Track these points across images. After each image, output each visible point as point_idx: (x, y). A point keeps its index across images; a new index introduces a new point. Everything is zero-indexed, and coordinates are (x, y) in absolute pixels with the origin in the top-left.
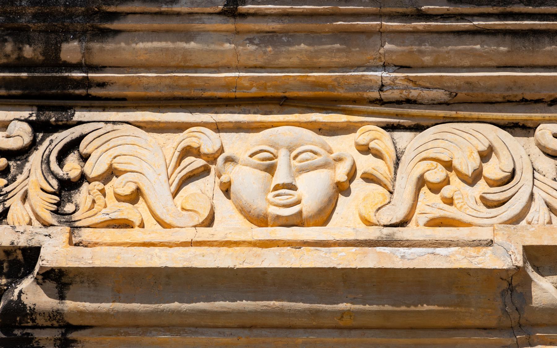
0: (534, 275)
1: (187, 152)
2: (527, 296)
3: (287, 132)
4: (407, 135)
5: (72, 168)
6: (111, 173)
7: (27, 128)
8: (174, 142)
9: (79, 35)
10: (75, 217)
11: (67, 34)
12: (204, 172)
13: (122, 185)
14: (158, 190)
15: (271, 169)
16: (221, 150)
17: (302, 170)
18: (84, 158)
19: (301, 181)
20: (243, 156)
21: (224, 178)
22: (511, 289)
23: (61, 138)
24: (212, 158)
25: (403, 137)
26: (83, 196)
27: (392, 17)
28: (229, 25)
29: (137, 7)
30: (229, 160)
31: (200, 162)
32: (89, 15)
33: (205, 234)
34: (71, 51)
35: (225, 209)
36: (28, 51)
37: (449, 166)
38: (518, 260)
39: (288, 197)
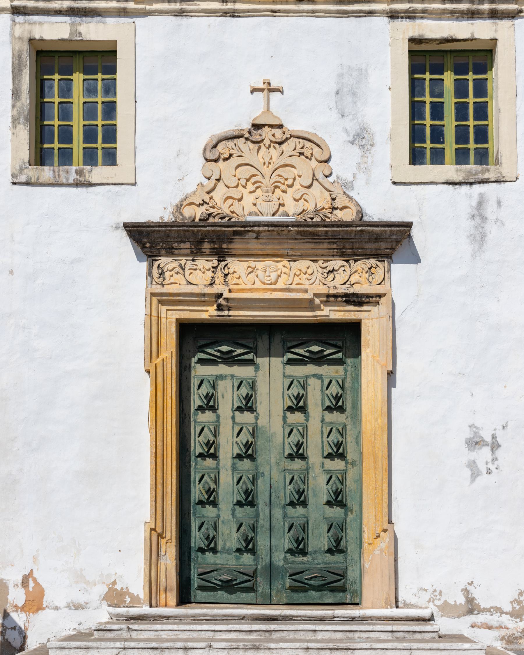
0: (315, 298)
1: (249, 267)
2: (314, 302)
3: (269, 263)
4: (293, 262)
5: (226, 271)
6: (234, 272)
7: (217, 261)
8: (246, 264)
9: (226, 243)
10: (228, 282)
11: (223, 242)
12: (252, 272)
13: (236, 275)
14: (243, 276)
15: (265, 272)
16: (256, 267)
17: (272, 272)
18: (229, 268)
19: (272, 274)
20: (260, 268)
21: (256, 274)
22: (311, 301)
23: (224, 263)
24: (254, 269)
25: (292, 263)
26: (229, 277)
27: (290, 239)
28: (257, 241)
29: (237, 237)
30: (257, 269)
31: (251, 270)
32: (228, 239)
33: (253, 287)
34: (224, 246)
35: (257, 280)
36: (216, 246)
37: (301, 270)
38: (312, 296)
39: (269, 278)
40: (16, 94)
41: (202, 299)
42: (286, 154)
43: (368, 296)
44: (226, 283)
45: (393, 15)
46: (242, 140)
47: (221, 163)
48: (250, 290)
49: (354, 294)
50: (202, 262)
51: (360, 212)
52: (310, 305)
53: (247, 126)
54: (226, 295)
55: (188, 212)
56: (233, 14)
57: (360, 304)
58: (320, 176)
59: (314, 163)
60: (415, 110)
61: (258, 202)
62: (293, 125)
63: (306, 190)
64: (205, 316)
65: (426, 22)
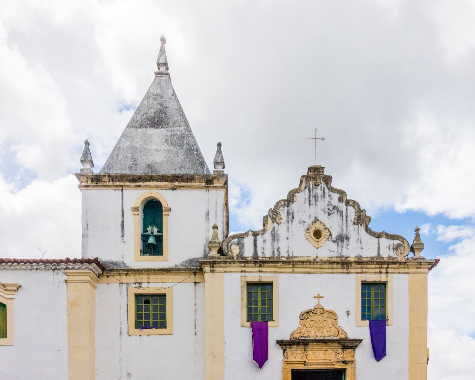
40: (242, 299)
41: (299, 363)
42: (325, 317)
43: (349, 361)
44: (306, 358)
45: (357, 273)
46: (311, 313)
47: (305, 320)
48: (314, 360)
49: (345, 361)
50: (299, 351)
51: (346, 335)
52: (332, 364)
53: (313, 308)
54: (307, 362)
55: (295, 336)
56: (309, 273)
57: (346, 364)
58: (335, 324)
59: (333, 320)
60: (363, 302)
61: (316, 332)
62: (326, 308)
63: (330, 329)
64: (300, 368)
65: (367, 275)
